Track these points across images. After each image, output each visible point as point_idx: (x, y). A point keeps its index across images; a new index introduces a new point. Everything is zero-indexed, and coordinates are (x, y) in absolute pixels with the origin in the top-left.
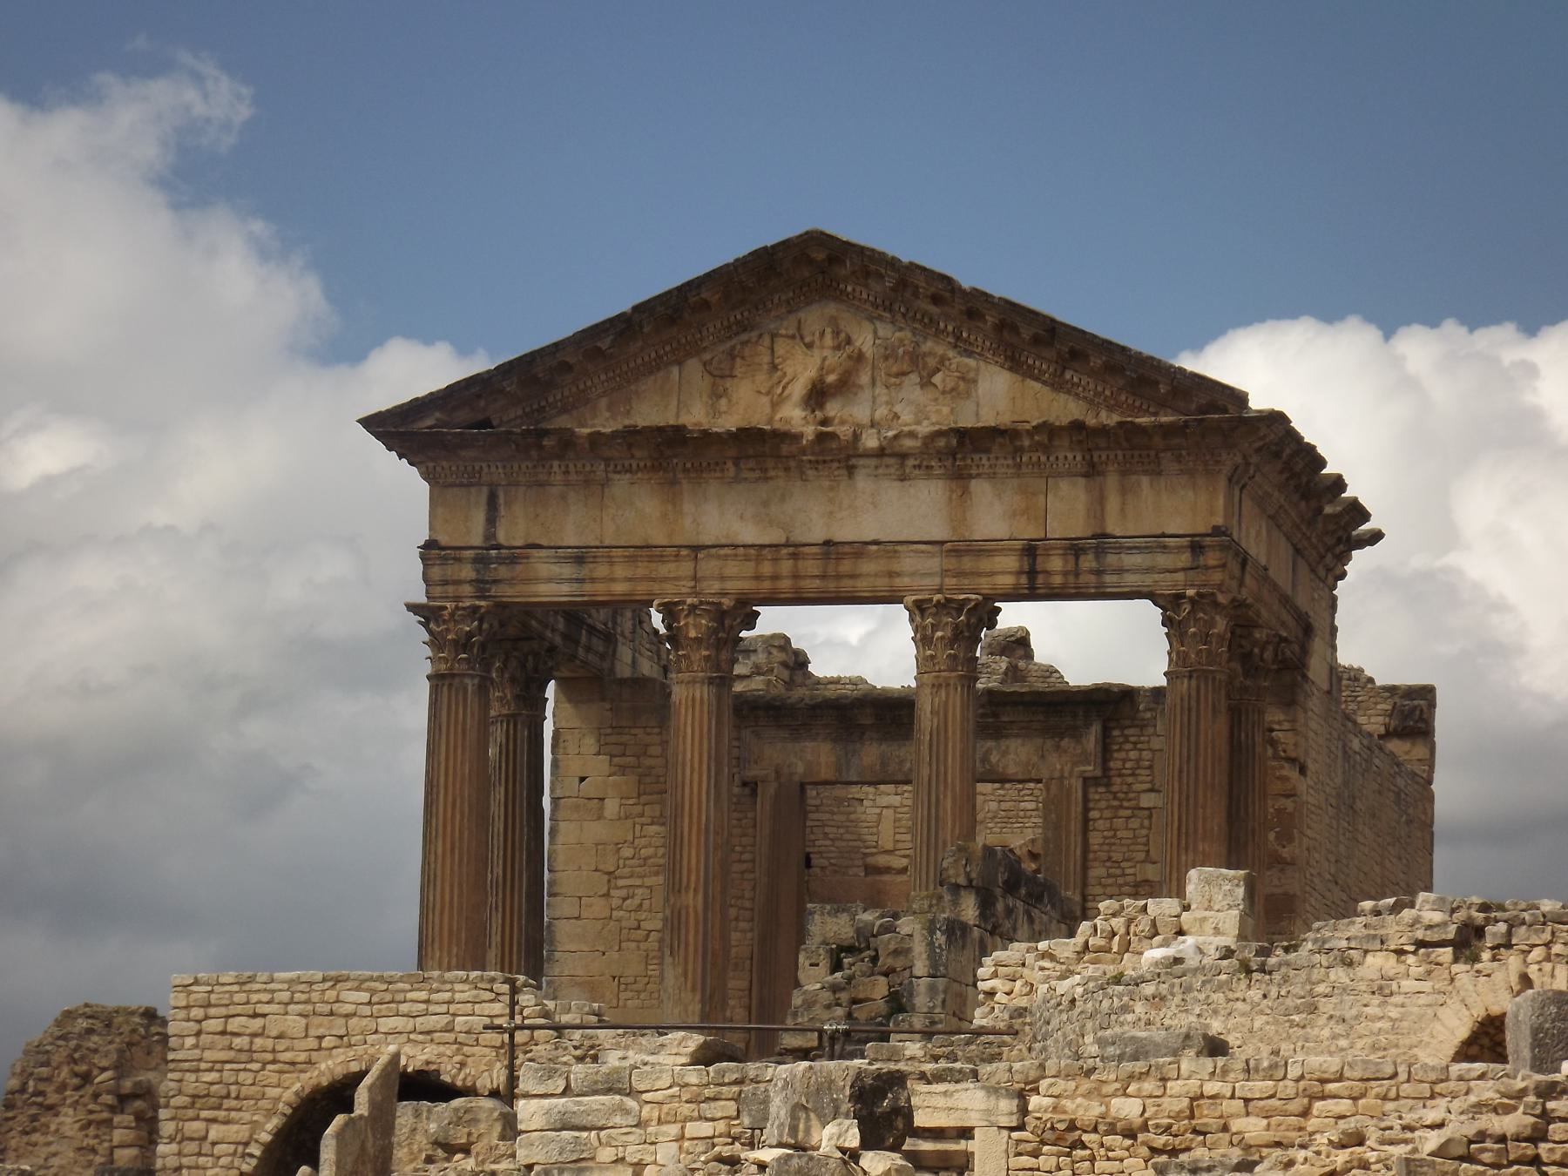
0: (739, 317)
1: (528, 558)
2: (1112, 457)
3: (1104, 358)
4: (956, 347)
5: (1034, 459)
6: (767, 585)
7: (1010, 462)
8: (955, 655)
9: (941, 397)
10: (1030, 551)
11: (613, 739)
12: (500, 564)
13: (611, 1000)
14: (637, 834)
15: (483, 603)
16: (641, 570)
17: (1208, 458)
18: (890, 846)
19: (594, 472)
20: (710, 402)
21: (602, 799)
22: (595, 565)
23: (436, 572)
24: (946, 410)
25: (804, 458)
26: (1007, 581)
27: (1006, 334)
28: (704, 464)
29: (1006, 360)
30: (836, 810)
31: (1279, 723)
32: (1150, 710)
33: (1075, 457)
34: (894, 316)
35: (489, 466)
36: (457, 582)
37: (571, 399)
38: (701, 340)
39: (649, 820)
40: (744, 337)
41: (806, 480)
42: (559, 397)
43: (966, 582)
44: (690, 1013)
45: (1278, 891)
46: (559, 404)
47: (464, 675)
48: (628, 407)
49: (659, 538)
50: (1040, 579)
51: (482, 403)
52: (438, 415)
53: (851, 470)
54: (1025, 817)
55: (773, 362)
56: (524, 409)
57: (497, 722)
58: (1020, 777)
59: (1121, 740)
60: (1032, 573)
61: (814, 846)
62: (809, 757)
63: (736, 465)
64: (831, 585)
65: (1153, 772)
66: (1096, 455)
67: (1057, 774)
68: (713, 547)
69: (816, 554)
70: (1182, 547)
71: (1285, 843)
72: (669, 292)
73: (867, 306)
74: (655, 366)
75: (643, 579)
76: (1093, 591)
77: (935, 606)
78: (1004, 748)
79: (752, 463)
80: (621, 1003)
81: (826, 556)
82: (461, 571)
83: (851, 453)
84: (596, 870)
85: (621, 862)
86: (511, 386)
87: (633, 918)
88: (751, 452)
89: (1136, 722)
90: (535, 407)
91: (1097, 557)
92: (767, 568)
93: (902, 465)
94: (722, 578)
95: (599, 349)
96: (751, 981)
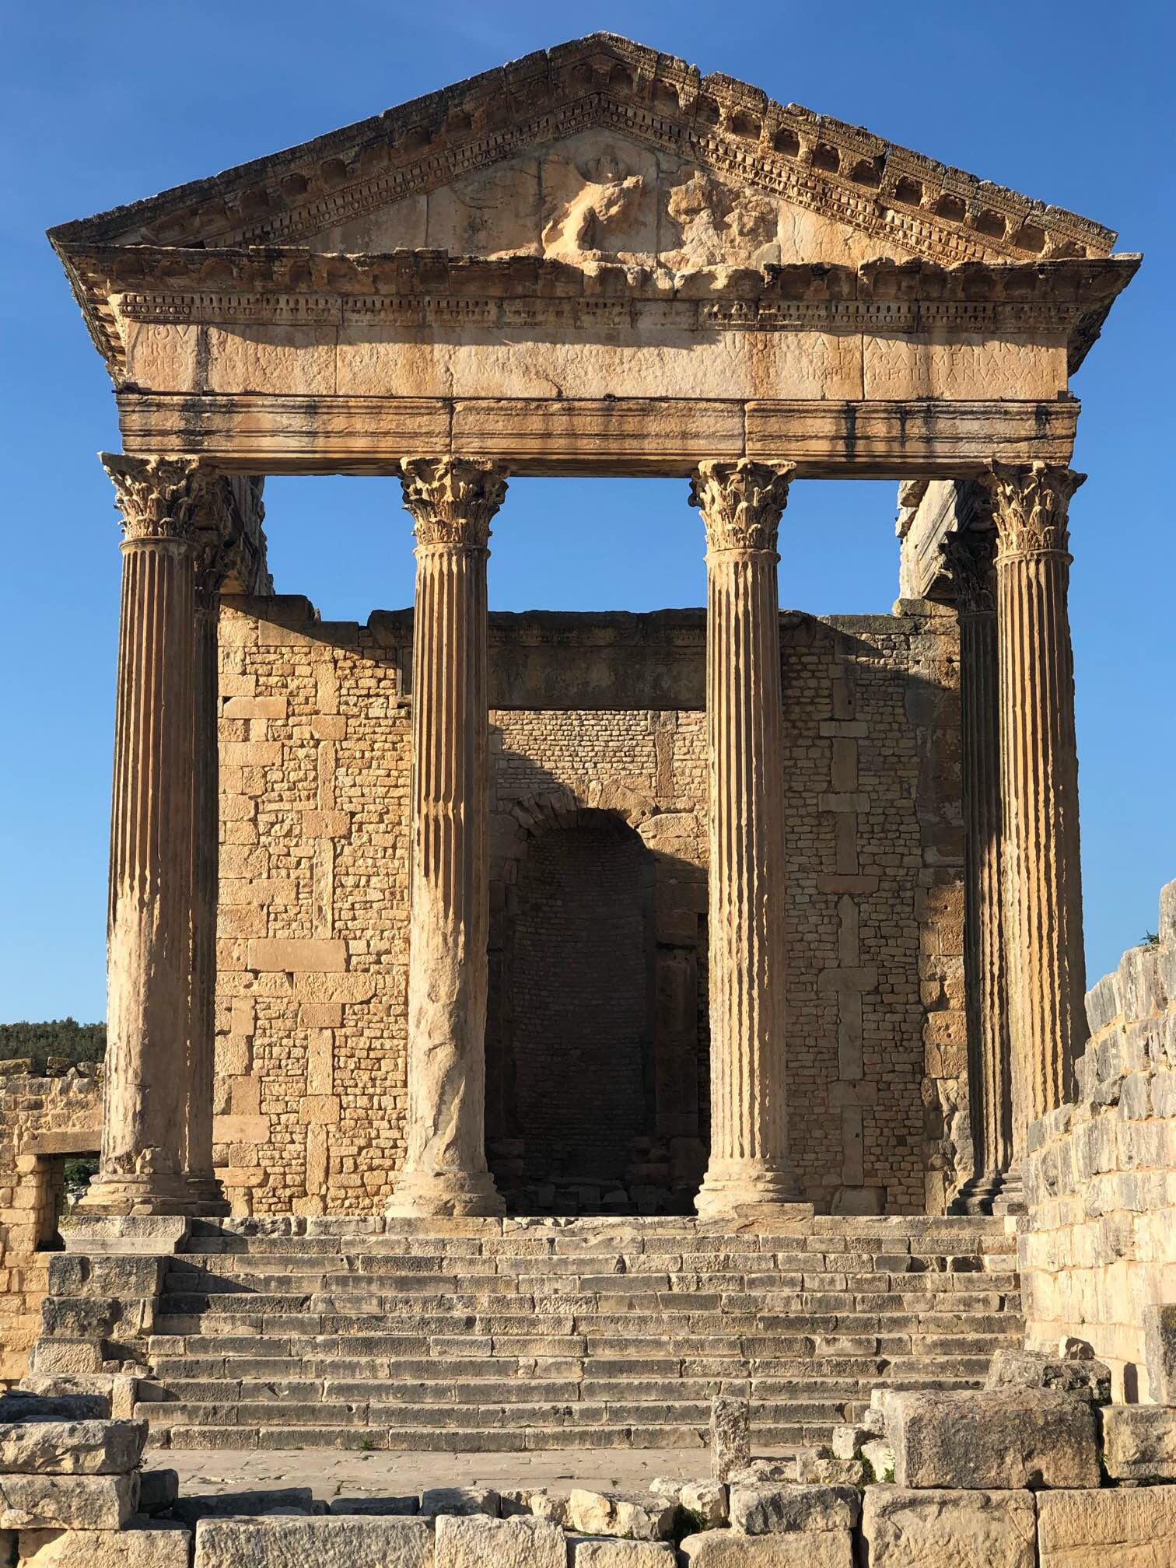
0: (500, 140)
1: (249, 406)
2: (942, 309)
3: (943, 193)
4: (753, 183)
5: (852, 310)
6: (534, 445)
7: (823, 313)
8: (762, 530)
9: (738, 239)
10: (849, 412)
11: (259, 658)
12: (214, 413)
14: (286, 757)
15: (195, 457)
16: (388, 422)
17: (1053, 313)
19: (329, 310)
20: (466, 235)
22: (330, 417)
23: (135, 421)
24: (743, 254)
25: (581, 300)
26: (821, 447)
27: (818, 171)
28: (462, 304)
29: (813, 199)
32: (826, 638)
33: (899, 308)
34: (680, 148)
35: (202, 299)
36: (164, 433)
37: (300, 226)
38: (454, 165)
39: (299, 742)
40: (505, 164)
41: (581, 328)
42: (286, 222)
43: (772, 446)
46: (286, 230)
47: (170, 541)
48: (366, 239)
49: (402, 386)
50: (860, 446)
51: (197, 221)
52: (143, 230)
53: (634, 316)
55: (540, 194)
56: (244, 234)
59: (799, 667)
60: (851, 439)
63: (500, 307)
64: (614, 446)
65: (832, 700)
66: (924, 305)
68: (470, 399)
69: (598, 410)
70: (1027, 413)
72: (429, 97)
73: (650, 135)
74: (399, 194)
75: (386, 434)
76: (921, 460)
77: (740, 472)
79: (518, 305)
80: (271, 933)
81: (607, 412)
82: (167, 420)
83: (637, 294)
84: (242, 794)
86: (234, 200)
87: (281, 845)
88: (520, 290)
89: (812, 650)
90: (258, 232)
91: (926, 423)
92: (535, 424)
93: (696, 313)
94: (482, 435)
95: (341, 164)
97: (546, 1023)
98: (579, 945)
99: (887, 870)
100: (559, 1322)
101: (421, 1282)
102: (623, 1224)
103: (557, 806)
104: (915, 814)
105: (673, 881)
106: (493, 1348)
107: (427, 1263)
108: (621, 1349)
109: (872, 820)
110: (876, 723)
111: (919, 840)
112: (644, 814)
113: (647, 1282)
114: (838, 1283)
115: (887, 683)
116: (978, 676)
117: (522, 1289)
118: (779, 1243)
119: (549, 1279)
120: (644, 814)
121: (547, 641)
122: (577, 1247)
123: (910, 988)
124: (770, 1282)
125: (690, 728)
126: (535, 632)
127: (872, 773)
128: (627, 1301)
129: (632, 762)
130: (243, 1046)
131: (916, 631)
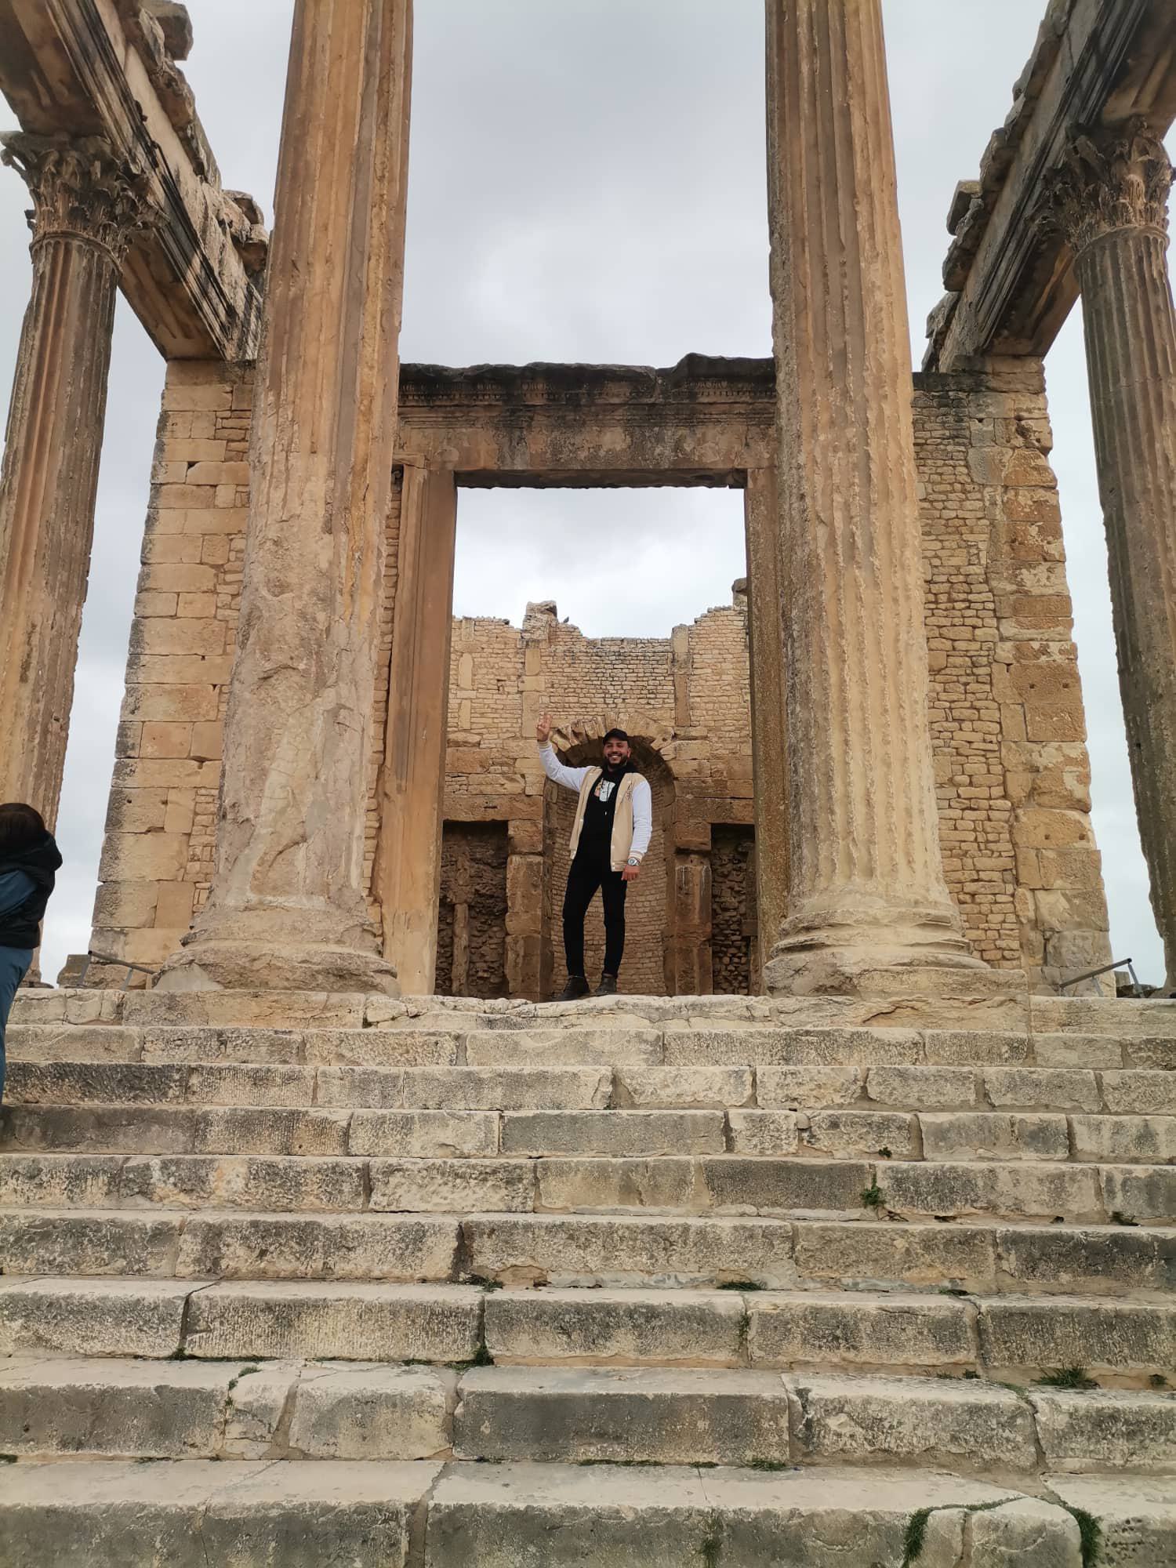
13: (208, 711)
18: (467, 726)
21: (215, 486)
31: (1029, 411)
44: (306, 496)
45: (1051, 591)
57: (41, 247)
58: (721, 466)
62: (466, 444)
67: (765, 464)
71: (1050, 538)
78: (699, 436)
84: (201, 564)
85: (232, 556)
96: (388, 691)
99: (956, 644)
100: (415, 1239)
101: (106, 1124)
102: (620, 1007)
103: (590, 733)
104: (986, 582)
105: (689, 797)
106: (187, 1329)
107: (155, 1080)
108: (591, 1342)
109: (935, 588)
110: (933, 483)
111: (994, 611)
112: (664, 740)
113: (679, 1130)
114: (1162, 1138)
115: (945, 442)
116: (1121, 310)
117: (360, 1141)
118: (973, 1048)
119: (425, 1120)
120: (664, 740)
121: (554, 400)
122: (515, 1050)
123: (995, 779)
124: (987, 1135)
125: (706, 671)
126: (540, 386)
127: (934, 537)
128: (615, 1180)
130: (176, 846)
131: (976, 389)
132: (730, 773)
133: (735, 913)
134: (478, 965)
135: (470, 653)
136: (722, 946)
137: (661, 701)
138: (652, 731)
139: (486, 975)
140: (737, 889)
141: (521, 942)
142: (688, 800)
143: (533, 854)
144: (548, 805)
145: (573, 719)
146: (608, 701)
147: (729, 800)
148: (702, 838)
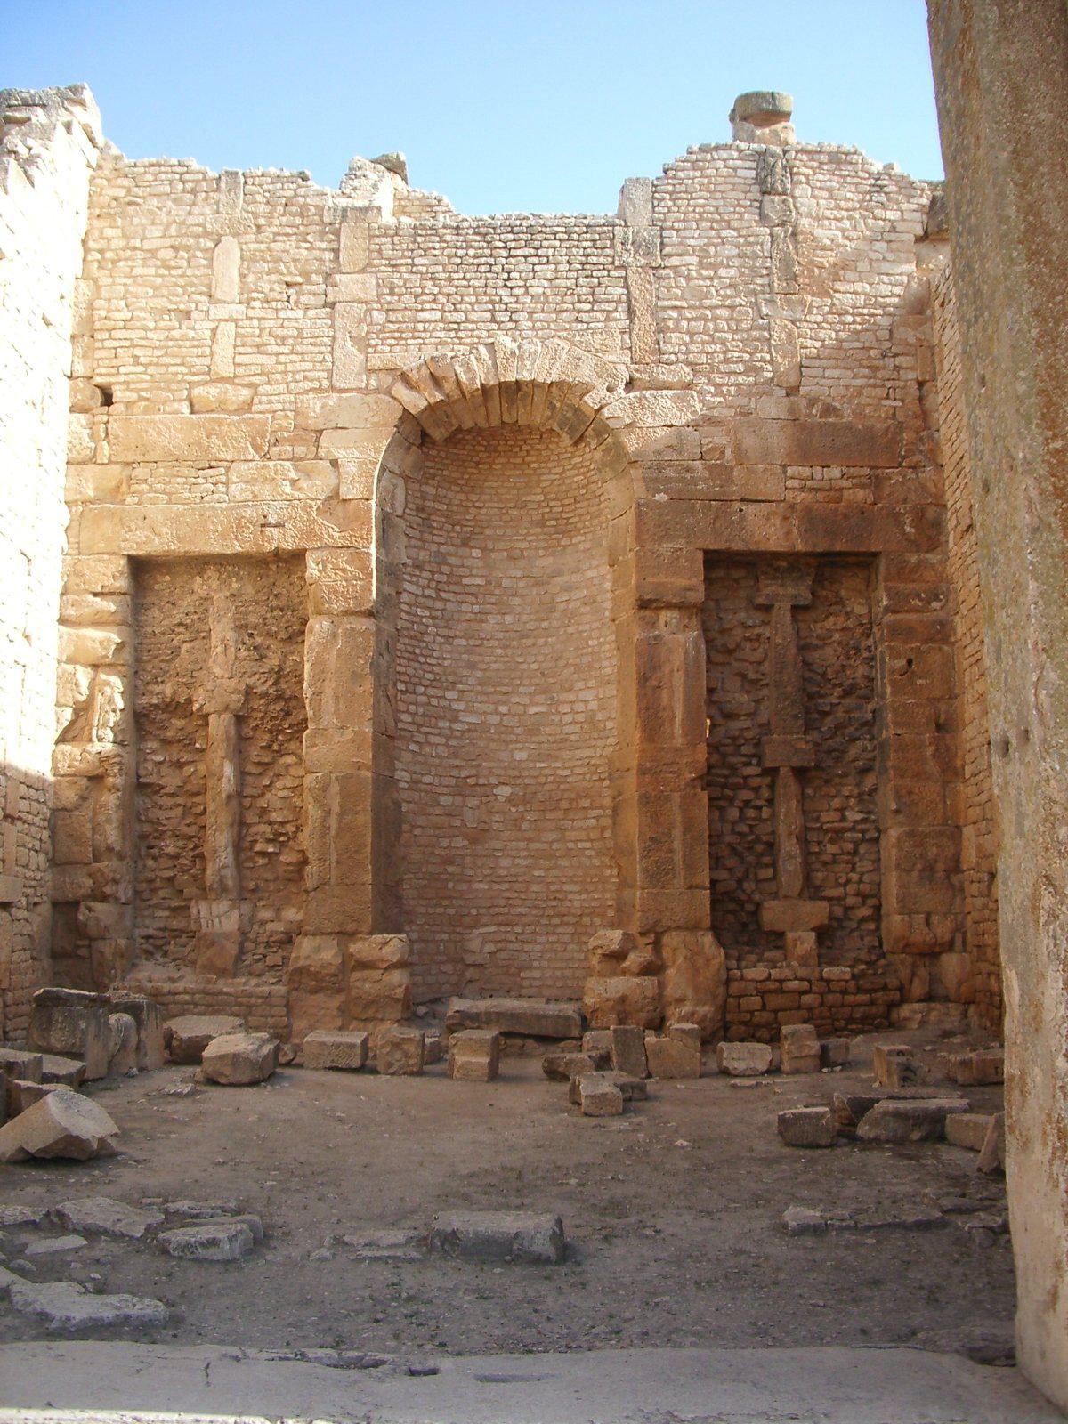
18: (226, 370)
30: (152, 325)
54: (425, 330)
61: (118, 373)
97: (453, 742)
98: (508, 619)
105: (662, 497)
129: (592, 310)
132: (739, 451)
133: (748, 723)
134: (254, 829)
135: (235, 235)
136: (724, 786)
137: (601, 316)
138: (585, 374)
139: (271, 850)
140: (752, 676)
141: (335, 788)
142: (659, 505)
143: (354, 613)
144: (385, 520)
145: (428, 352)
146: (502, 317)
147: (736, 506)
148: (689, 581)
